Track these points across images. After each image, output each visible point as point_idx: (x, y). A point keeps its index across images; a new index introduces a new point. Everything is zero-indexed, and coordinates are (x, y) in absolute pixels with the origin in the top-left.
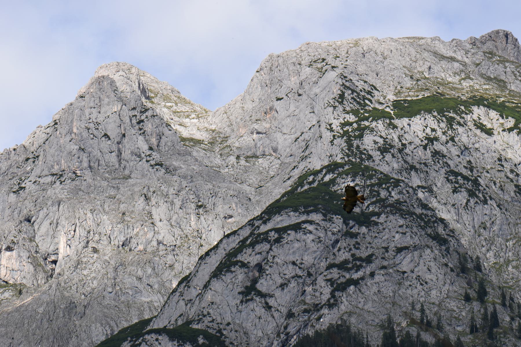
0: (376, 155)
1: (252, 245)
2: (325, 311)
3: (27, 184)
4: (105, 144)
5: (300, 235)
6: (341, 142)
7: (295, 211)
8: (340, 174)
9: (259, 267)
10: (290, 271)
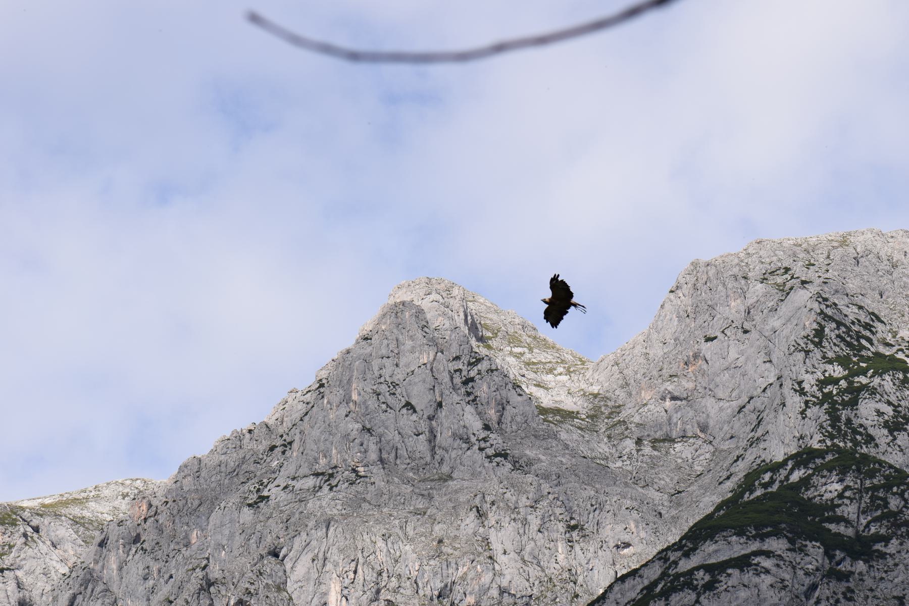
0: (881, 435)
3: (272, 491)
4: (408, 421)
5: (749, 577)
6: (818, 413)
7: (739, 534)
8: (818, 470)
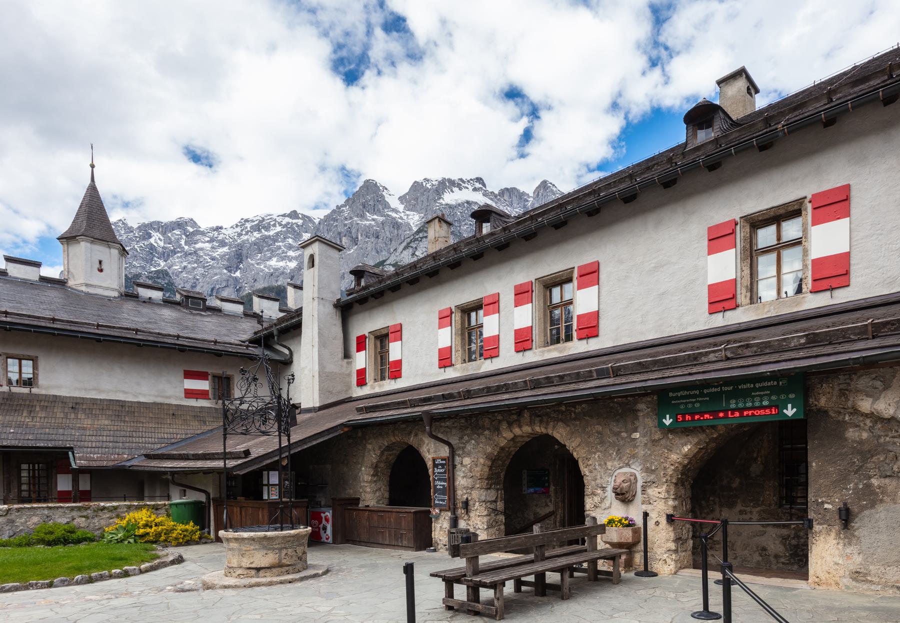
1: (414, 241)
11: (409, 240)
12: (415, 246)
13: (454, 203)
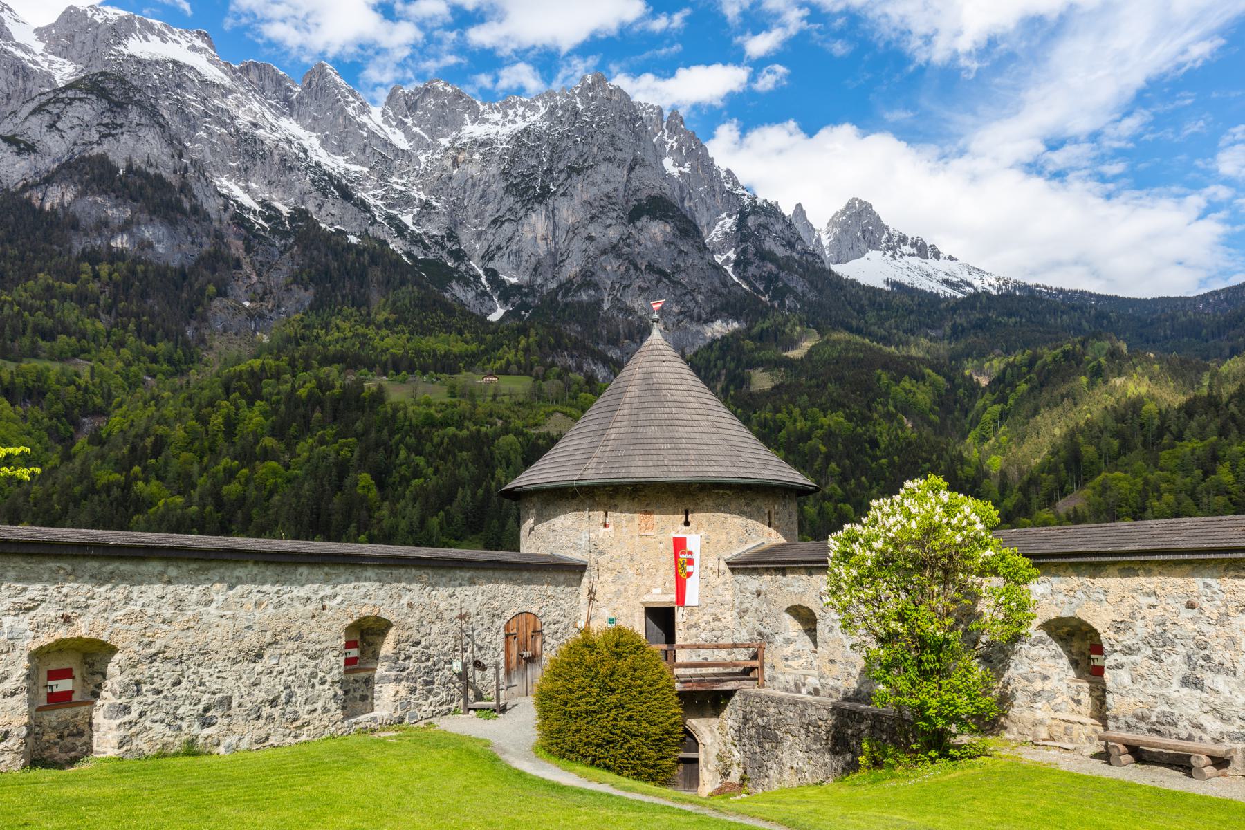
1: (55, 103)
2: (95, 146)
9: (59, 116)
10: (76, 122)
11: (44, 99)
12: (56, 111)
13: (147, 57)
